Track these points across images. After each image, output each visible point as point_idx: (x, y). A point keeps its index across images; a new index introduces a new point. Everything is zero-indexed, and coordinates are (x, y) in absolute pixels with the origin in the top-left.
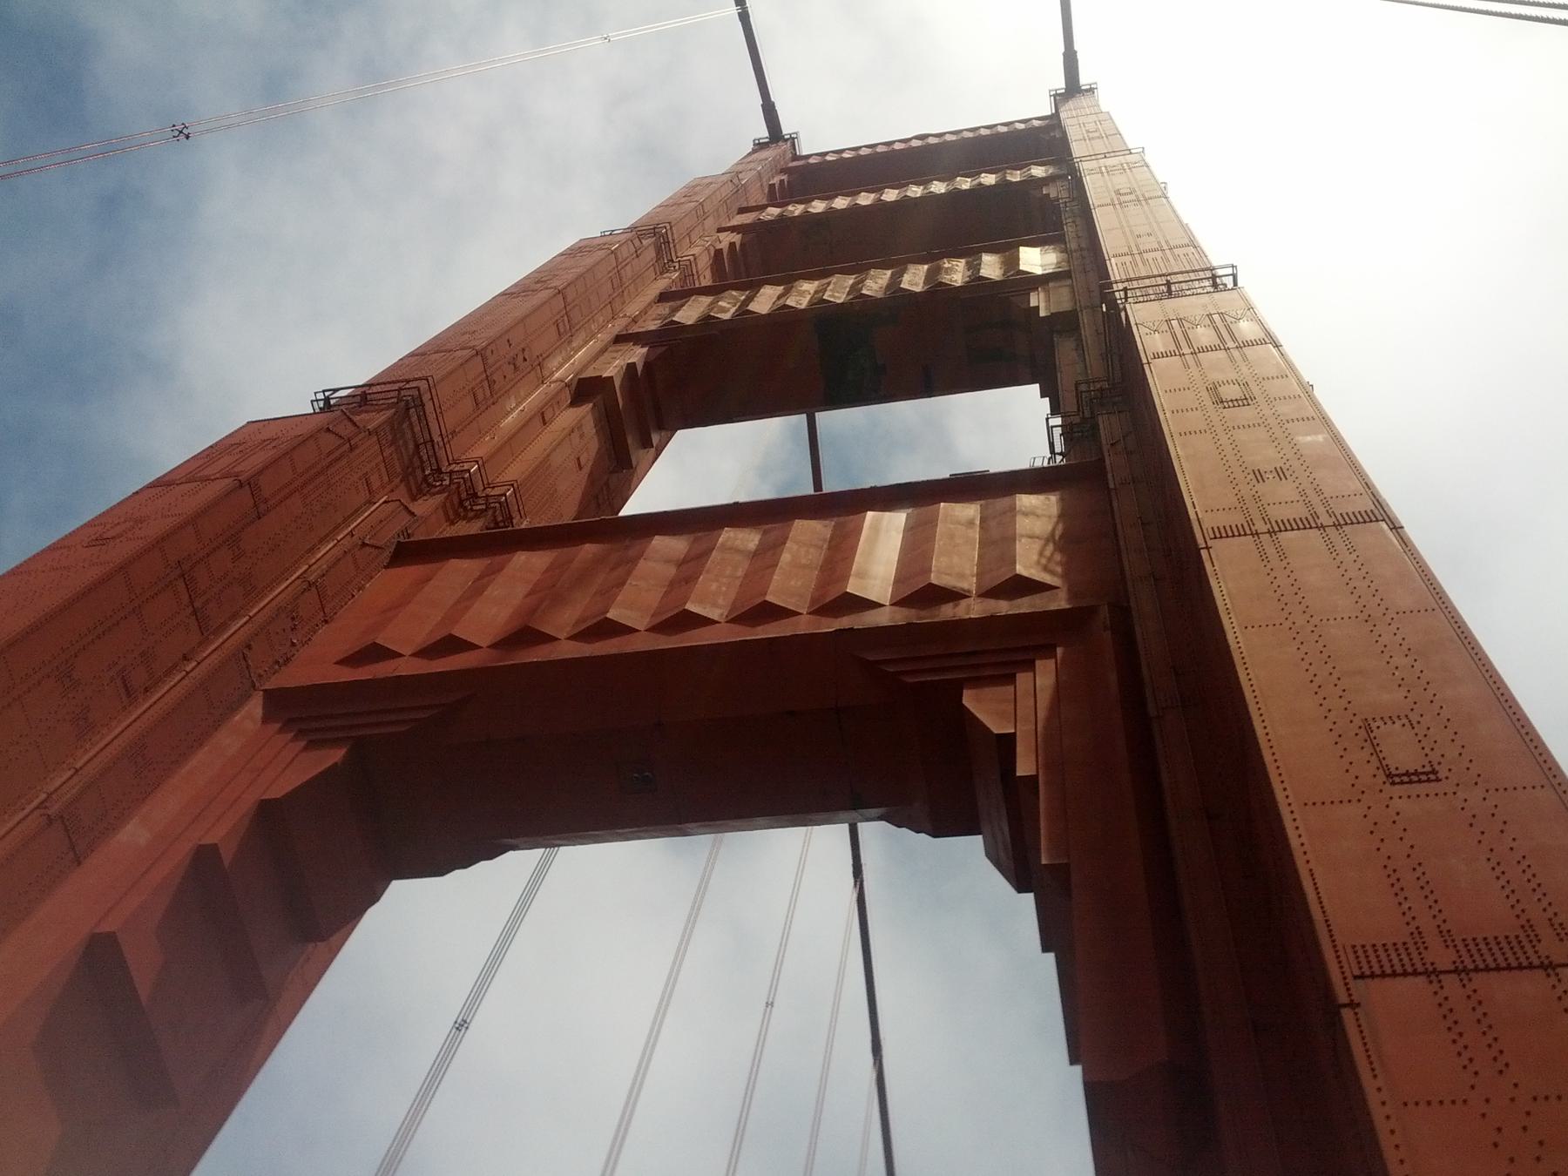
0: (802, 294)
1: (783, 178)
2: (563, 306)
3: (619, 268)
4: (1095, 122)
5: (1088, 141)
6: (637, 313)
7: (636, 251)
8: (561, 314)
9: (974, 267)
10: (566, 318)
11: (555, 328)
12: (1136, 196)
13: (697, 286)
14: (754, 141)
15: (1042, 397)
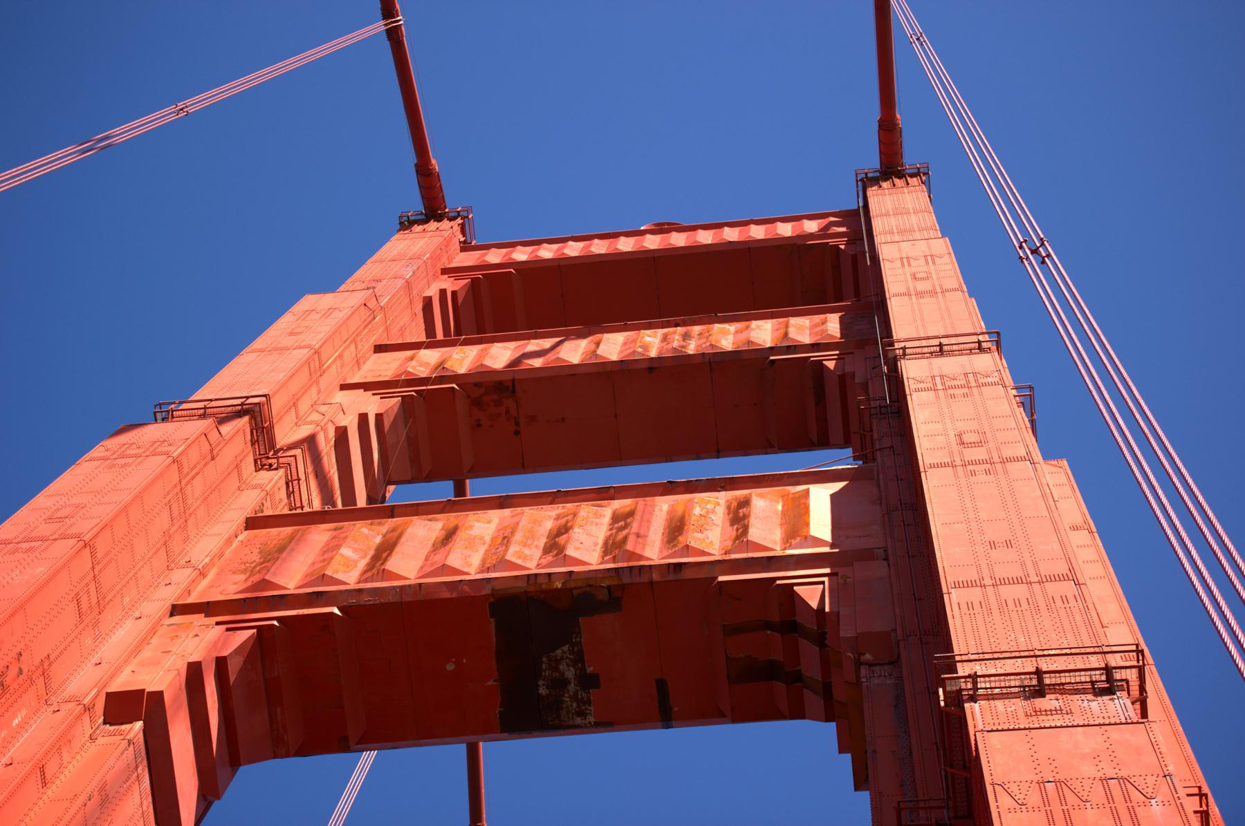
0: (471, 544)
1: (444, 286)
2: (91, 566)
3: (184, 482)
4: (926, 256)
5: (914, 297)
6: (207, 560)
7: (212, 451)
8: (86, 580)
9: (739, 517)
10: (92, 586)
11: (73, 605)
12: (989, 452)
13: (307, 509)
14: (401, 217)
15: (841, 751)
